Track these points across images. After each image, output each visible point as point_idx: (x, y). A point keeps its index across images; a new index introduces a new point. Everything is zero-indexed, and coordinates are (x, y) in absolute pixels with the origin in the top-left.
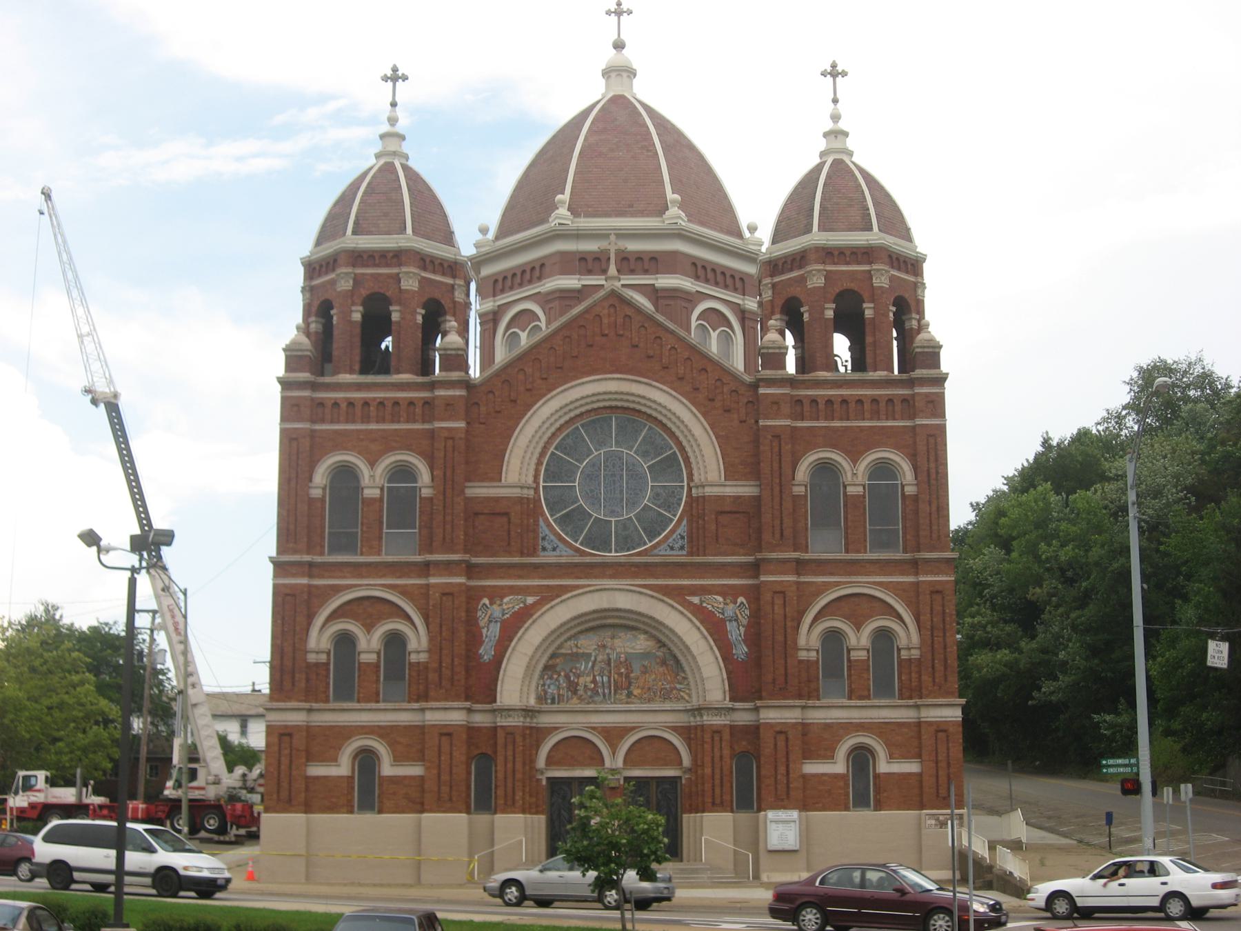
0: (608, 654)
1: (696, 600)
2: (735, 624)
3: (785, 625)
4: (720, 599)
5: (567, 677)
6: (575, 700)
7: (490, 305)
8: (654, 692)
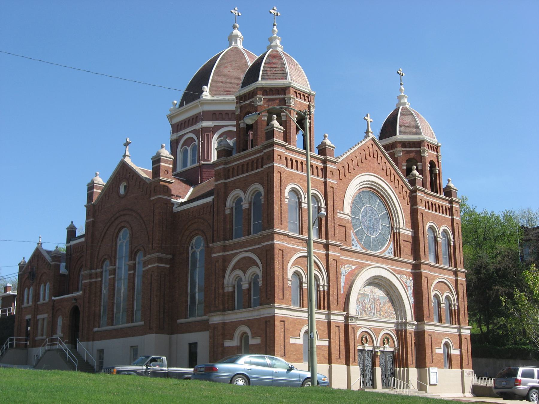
0: (374, 295)
1: (399, 276)
2: (410, 287)
3: (428, 291)
4: (405, 277)
5: (362, 304)
6: (365, 315)
7: (175, 136)
8: (387, 314)
